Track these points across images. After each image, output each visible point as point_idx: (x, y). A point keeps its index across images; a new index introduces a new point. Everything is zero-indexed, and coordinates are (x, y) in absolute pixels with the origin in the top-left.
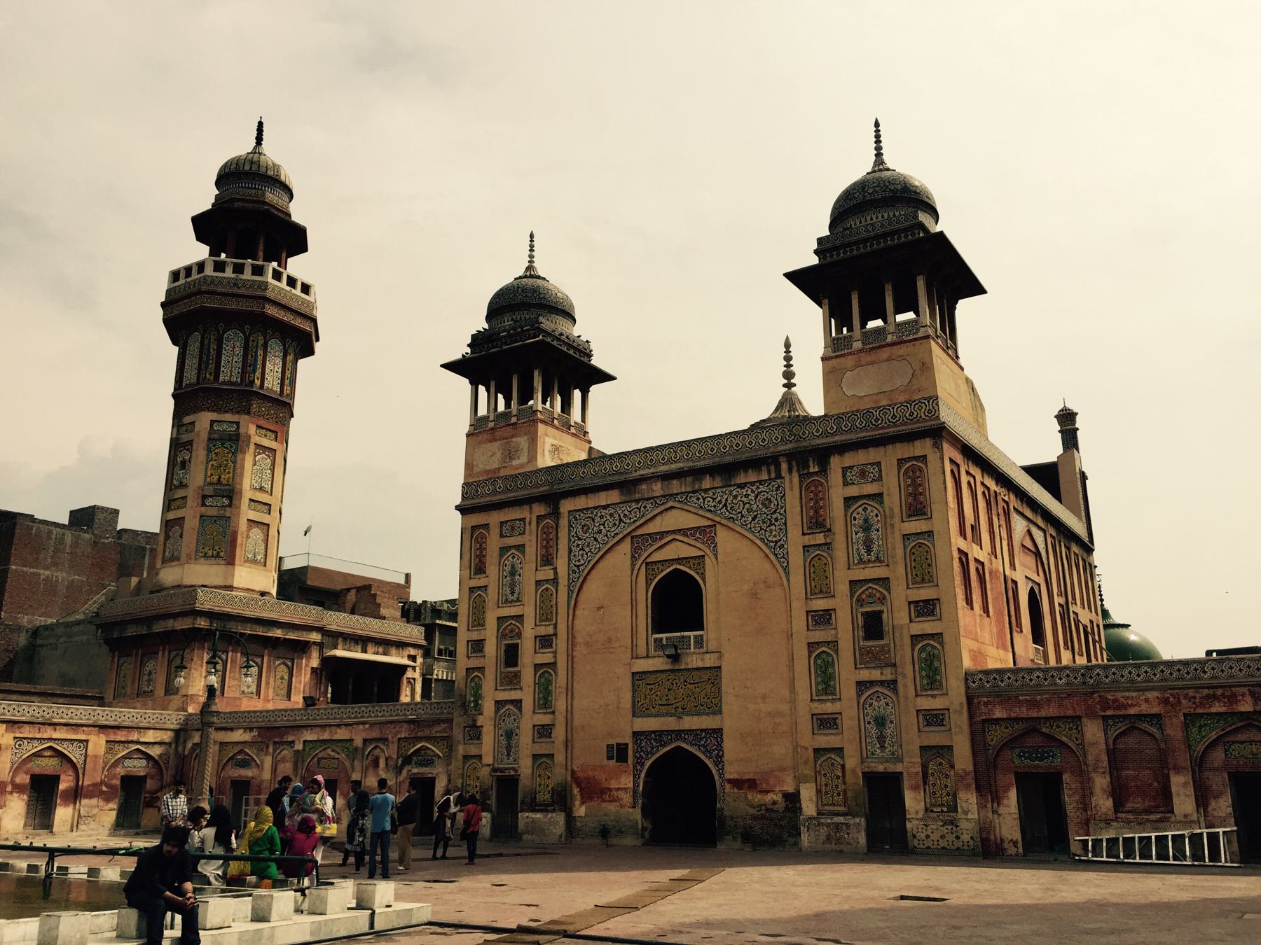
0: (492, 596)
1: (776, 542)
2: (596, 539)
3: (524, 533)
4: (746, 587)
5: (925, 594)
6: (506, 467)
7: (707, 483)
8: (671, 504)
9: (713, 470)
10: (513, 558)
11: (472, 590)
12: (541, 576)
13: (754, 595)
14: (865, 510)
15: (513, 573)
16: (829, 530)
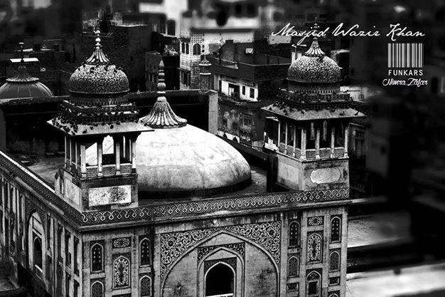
0: (109, 283)
1: (275, 252)
2: (177, 250)
3: (130, 245)
4: (258, 274)
5: (335, 275)
6: (115, 204)
7: (243, 221)
8: (222, 231)
9: (246, 216)
10: (121, 260)
11: (92, 280)
12: (143, 271)
13: (261, 277)
14: (314, 237)
15: (121, 269)
16: (300, 246)
